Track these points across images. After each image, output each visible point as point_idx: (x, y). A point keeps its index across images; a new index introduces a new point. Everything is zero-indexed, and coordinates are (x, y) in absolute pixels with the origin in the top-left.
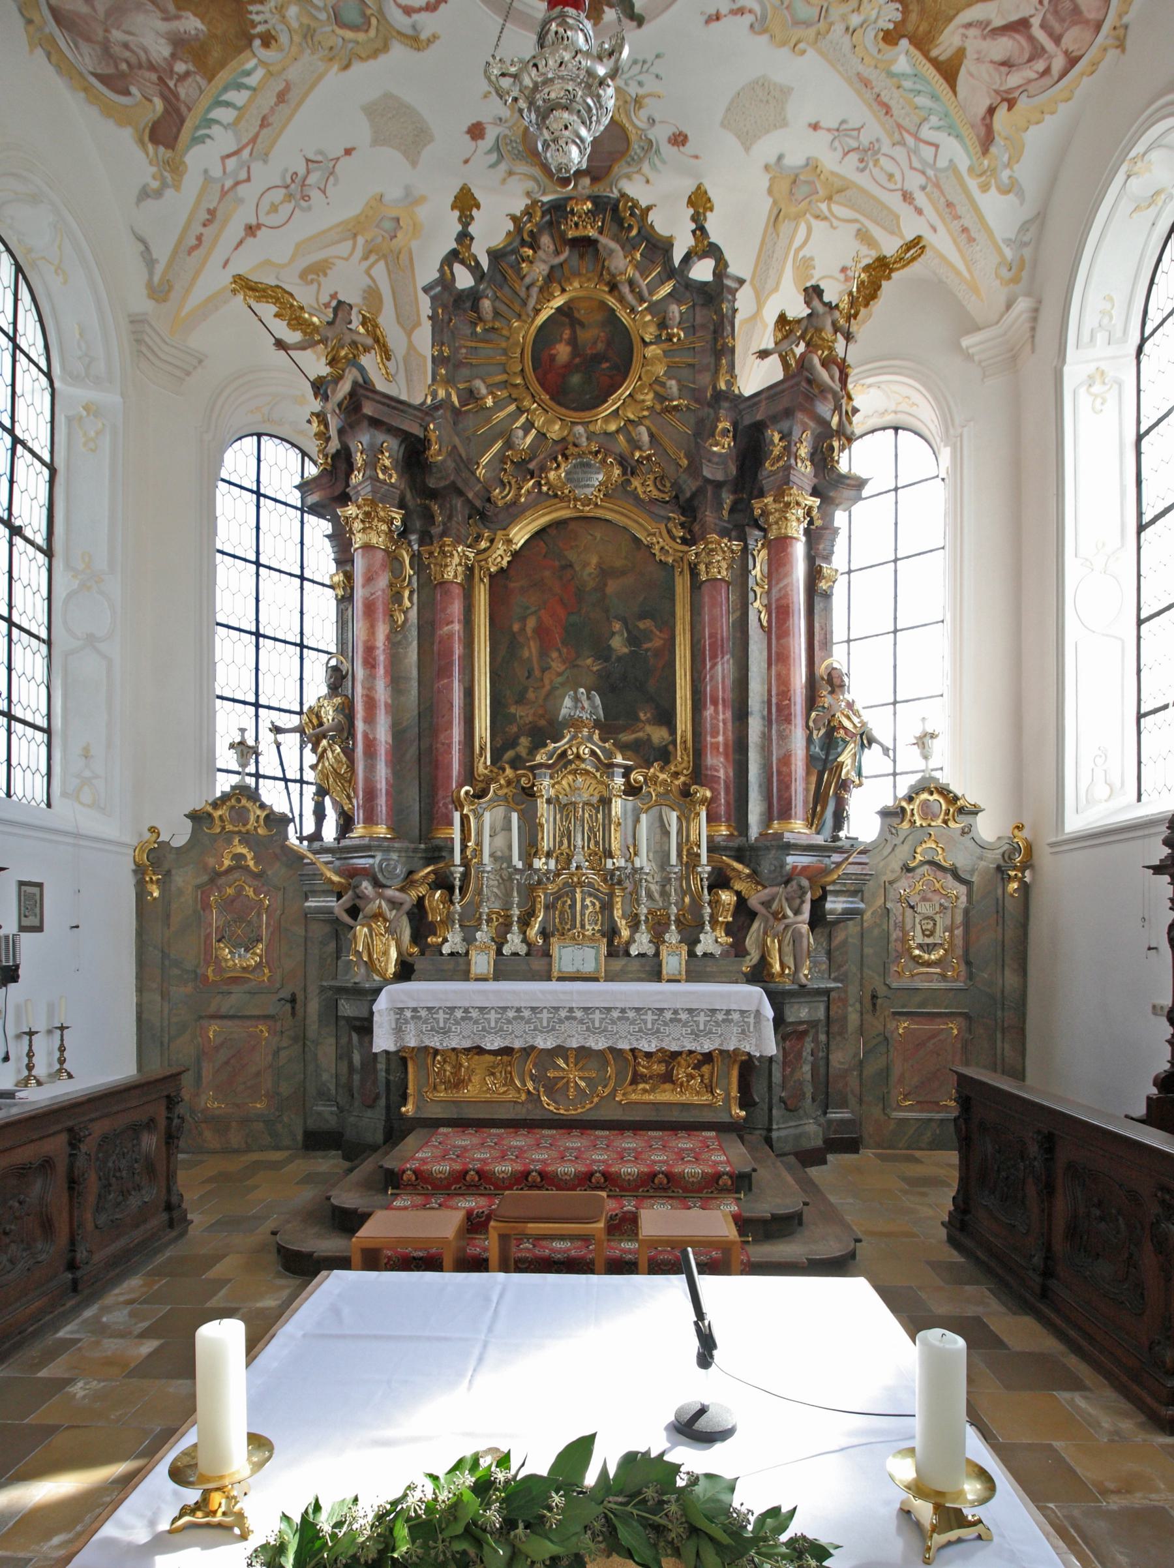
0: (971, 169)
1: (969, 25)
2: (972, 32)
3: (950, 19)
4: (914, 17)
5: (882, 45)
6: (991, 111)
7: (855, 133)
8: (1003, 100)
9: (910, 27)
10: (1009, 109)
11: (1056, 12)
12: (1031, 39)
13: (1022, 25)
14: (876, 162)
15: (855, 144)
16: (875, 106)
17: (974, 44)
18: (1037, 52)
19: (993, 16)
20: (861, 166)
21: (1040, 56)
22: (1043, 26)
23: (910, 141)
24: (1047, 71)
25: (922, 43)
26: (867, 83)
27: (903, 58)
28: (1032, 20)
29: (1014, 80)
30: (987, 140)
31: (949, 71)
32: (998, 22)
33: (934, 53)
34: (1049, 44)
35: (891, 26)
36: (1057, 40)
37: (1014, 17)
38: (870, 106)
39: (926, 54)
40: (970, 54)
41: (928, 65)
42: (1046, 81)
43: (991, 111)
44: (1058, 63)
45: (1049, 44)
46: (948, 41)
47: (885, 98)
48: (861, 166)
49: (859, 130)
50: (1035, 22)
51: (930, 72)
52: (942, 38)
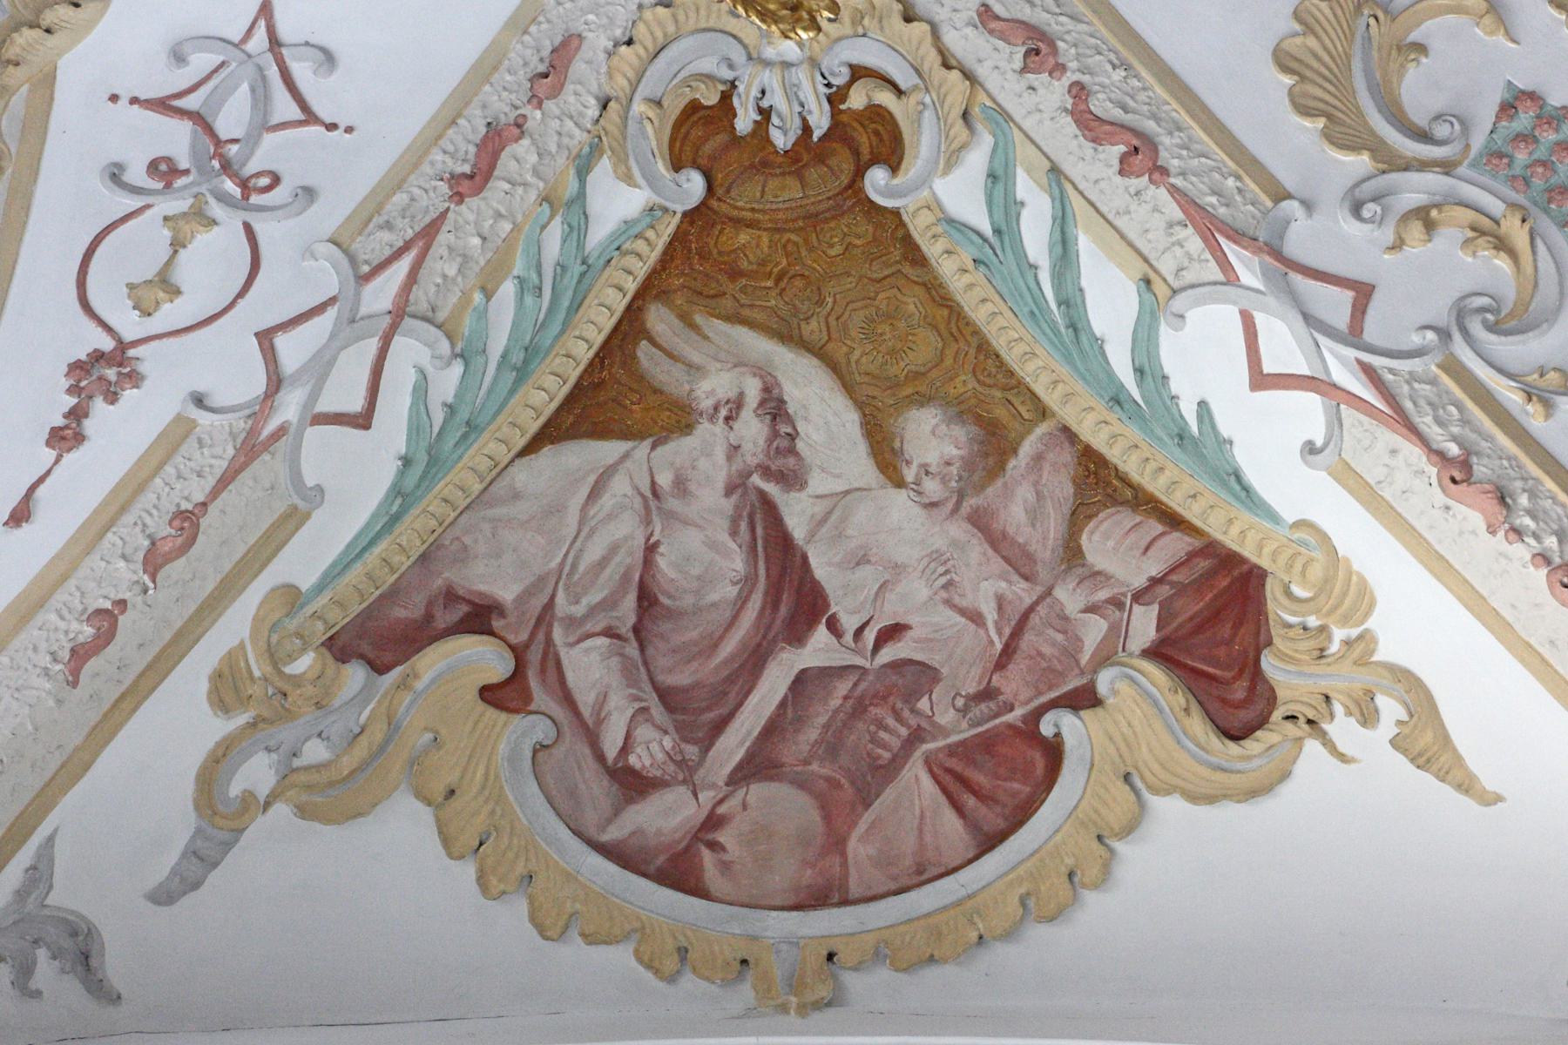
0: (290, 596)
1: (775, 409)
2: (752, 430)
3: (788, 336)
4: (786, 193)
5: (675, 107)
6: (479, 617)
7: (285, 108)
8: (519, 653)
9: (745, 197)
10: (489, 694)
11: (858, 708)
12: (754, 662)
13: (796, 599)
14: (200, 217)
15: (232, 120)
16: (473, 126)
17: (705, 457)
18: (695, 714)
19: (818, 483)
20: (137, 174)
21: (684, 732)
22: (802, 681)
23: (381, 294)
24: (632, 784)
25: (693, 264)
26: (551, 74)
27: (630, 201)
28: (821, 634)
29: (589, 667)
30: (379, 639)
31: (608, 398)
32: (797, 514)
33: (659, 319)
34: (733, 745)
35: (744, 122)
36: (758, 765)
37: (822, 567)
38: (449, 117)
39: (649, 290)
40: (680, 449)
41: (620, 304)
42: (596, 789)
43: (479, 617)
44: (665, 816)
45: (733, 745)
46: (718, 362)
47: (519, 157)
48: (137, 174)
49: (310, 117)
50: (819, 649)
51: (599, 321)
52: (717, 328)
